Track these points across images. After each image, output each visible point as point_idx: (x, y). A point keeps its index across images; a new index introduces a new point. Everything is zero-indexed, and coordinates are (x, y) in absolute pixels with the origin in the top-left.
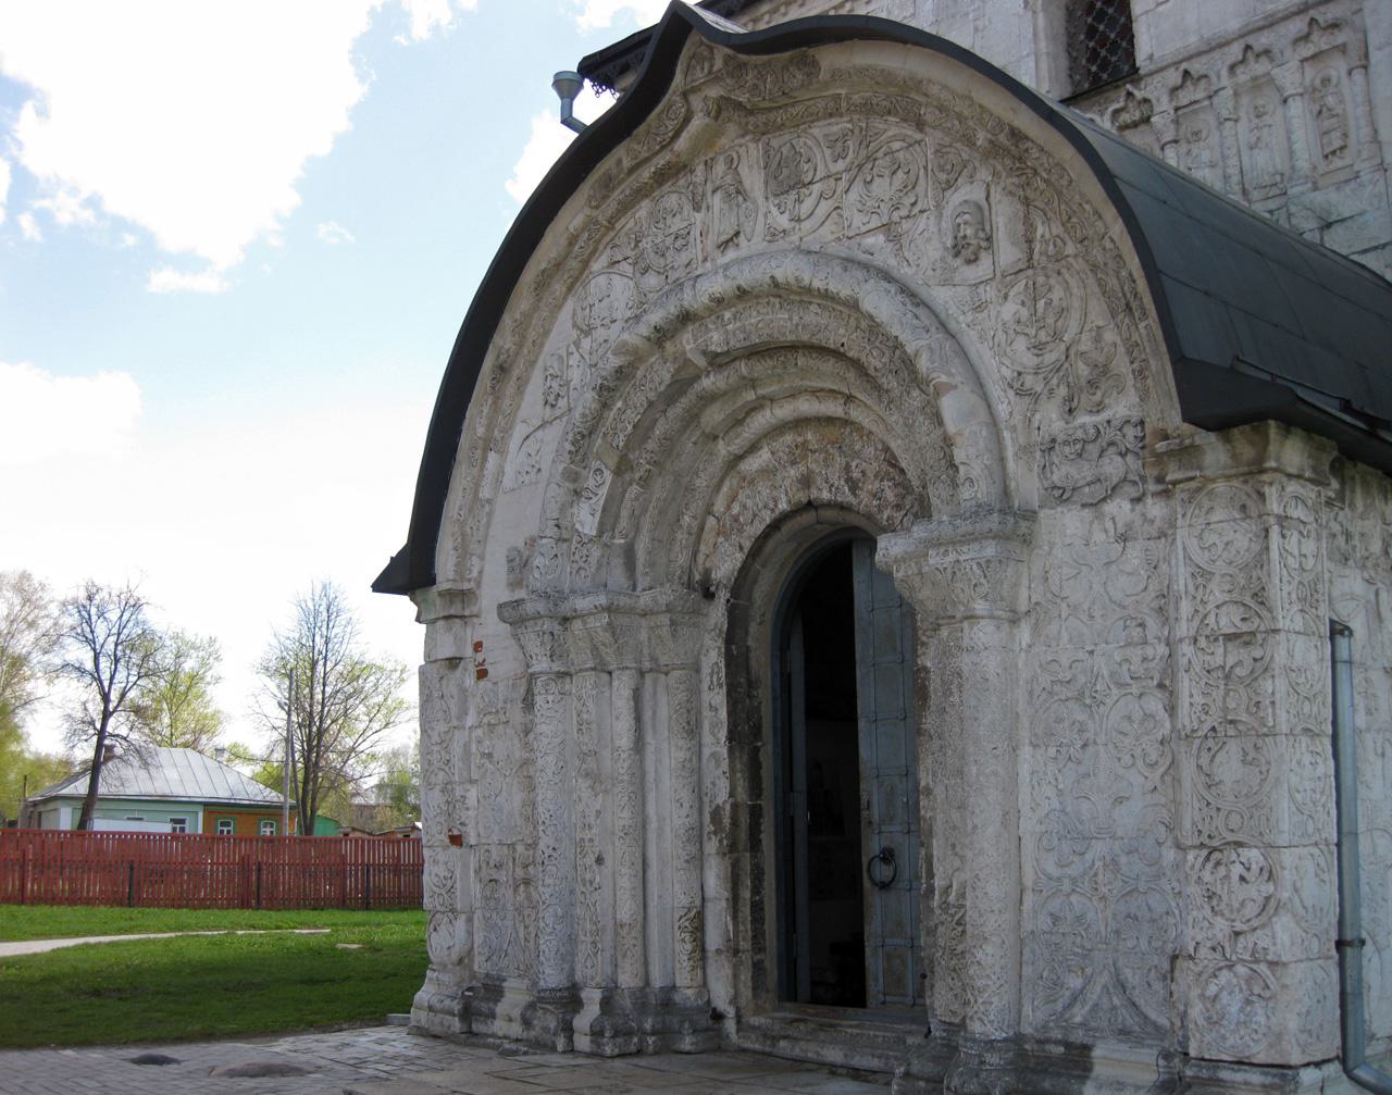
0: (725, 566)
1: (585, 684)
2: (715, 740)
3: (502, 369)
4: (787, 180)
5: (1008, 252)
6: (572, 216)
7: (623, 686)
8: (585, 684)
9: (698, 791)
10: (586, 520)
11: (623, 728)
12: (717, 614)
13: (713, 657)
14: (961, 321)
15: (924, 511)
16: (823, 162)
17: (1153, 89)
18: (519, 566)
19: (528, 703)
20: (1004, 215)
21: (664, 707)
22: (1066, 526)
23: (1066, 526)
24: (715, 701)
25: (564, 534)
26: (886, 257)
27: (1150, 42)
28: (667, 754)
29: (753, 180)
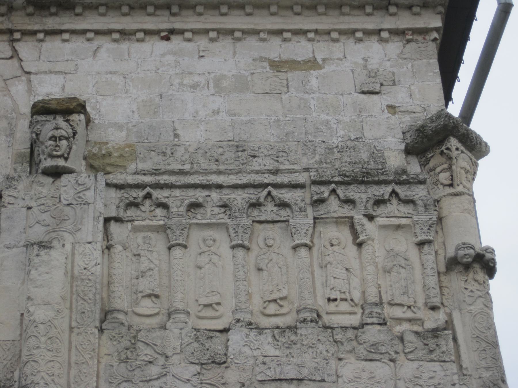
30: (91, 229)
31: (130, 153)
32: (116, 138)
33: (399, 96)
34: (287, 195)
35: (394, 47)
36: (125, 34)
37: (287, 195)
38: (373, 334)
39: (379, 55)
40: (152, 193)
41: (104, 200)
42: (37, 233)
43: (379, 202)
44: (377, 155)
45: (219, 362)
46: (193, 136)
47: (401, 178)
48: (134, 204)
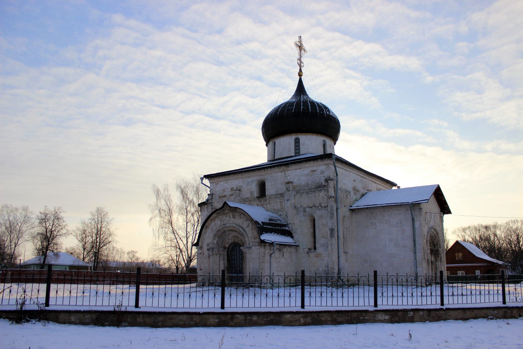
0: (227, 246)
1: (215, 256)
2: (226, 261)
3: (206, 227)
4: (234, 217)
5: (251, 228)
6: (214, 215)
7: (218, 256)
8: (215, 256)
9: (224, 265)
10: (215, 242)
11: (218, 260)
12: (226, 250)
13: (226, 254)
14: (247, 232)
15: (244, 245)
16: (237, 217)
17: (267, 198)
18: (208, 245)
19: (209, 257)
20: (250, 225)
21: (222, 258)
22: (254, 248)
23: (254, 248)
24: (226, 257)
25: (213, 243)
26: (242, 225)
27: (267, 193)
28: (222, 262)
29: (231, 216)
30: (293, 197)
31: (297, 186)
32: (295, 184)
33: (325, 174)
34: (312, 190)
35: (325, 166)
36: (296, 169)
37: (312, 190)
38: (320, 207)
39: (323, 168)
40: (299, 191)
41: (294, 193)
42: (288, 198)
43: (321, 190)
44: (322, 184)
45: (305, 212)
46: (303, 183)
47: (324, 186)
48: (297, 193)
